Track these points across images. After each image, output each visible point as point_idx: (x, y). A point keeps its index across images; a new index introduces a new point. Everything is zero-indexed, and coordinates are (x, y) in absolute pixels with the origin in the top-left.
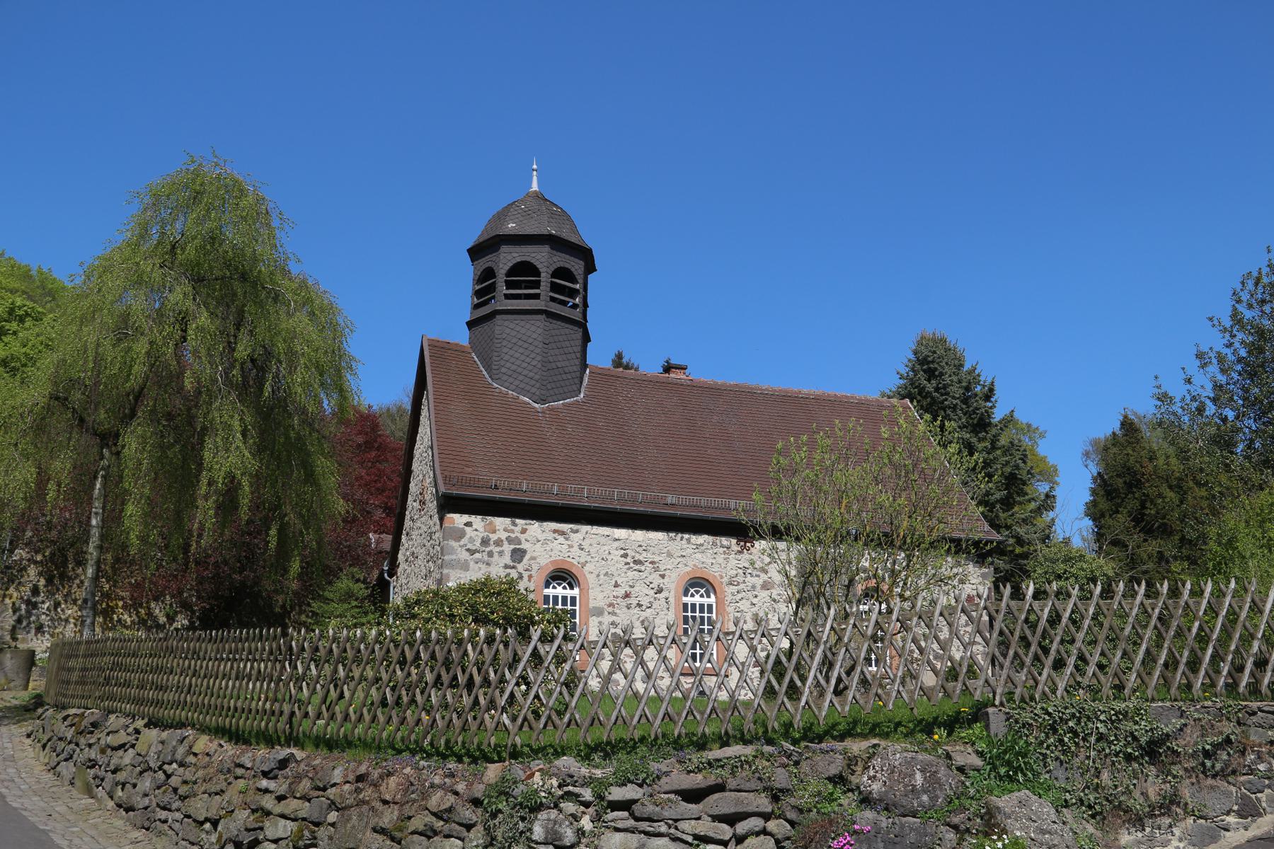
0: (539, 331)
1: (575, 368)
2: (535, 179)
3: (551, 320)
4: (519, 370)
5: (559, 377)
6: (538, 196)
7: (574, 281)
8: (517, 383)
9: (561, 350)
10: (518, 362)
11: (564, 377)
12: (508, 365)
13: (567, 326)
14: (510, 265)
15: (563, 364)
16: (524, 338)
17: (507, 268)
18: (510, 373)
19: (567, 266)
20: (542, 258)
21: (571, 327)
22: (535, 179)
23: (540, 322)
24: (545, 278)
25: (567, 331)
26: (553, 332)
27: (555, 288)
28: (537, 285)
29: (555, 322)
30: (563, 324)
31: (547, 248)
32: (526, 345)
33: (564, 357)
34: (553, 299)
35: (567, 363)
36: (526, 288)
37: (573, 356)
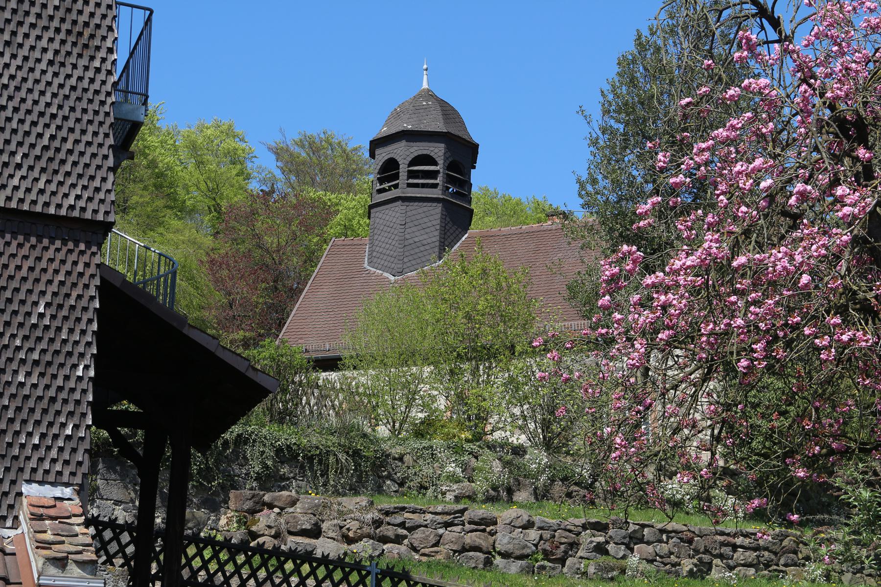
0: (398, 214)
1: (434, 239)
2: (425, 77)
3: (407, 204)
4: (385, 251)
5: (417, 250)
6: (429, 95)
7: (435, 163)
8: (382, 262)
9: (419, 227)
10: (384, 245)
11: (422, 249)
12: (378, 249)
13: (425, 204)
14: (381, 164)
15: (421, 238)
16: (388, 224)
17: (379, 167)
18: (378, 255)
19: (425, 152)
20: (403, 152)
21: (430, 204)
22: (425, 77)
23: (398, 206)
24: (403, 169)
25: (425, 209)
26: (409, 214)
27: (412, 174)
28: (396, 177)
29: (411, 204)
30: (421, 204)
31: (403, 143)
32: (389, 229)
33: (422, 232)
34: (410, 185)
35: (425, 237)
36: (423, 178)
37: (433, 229)
